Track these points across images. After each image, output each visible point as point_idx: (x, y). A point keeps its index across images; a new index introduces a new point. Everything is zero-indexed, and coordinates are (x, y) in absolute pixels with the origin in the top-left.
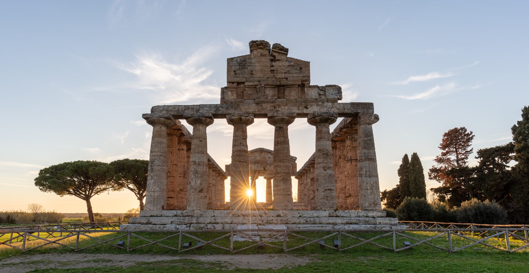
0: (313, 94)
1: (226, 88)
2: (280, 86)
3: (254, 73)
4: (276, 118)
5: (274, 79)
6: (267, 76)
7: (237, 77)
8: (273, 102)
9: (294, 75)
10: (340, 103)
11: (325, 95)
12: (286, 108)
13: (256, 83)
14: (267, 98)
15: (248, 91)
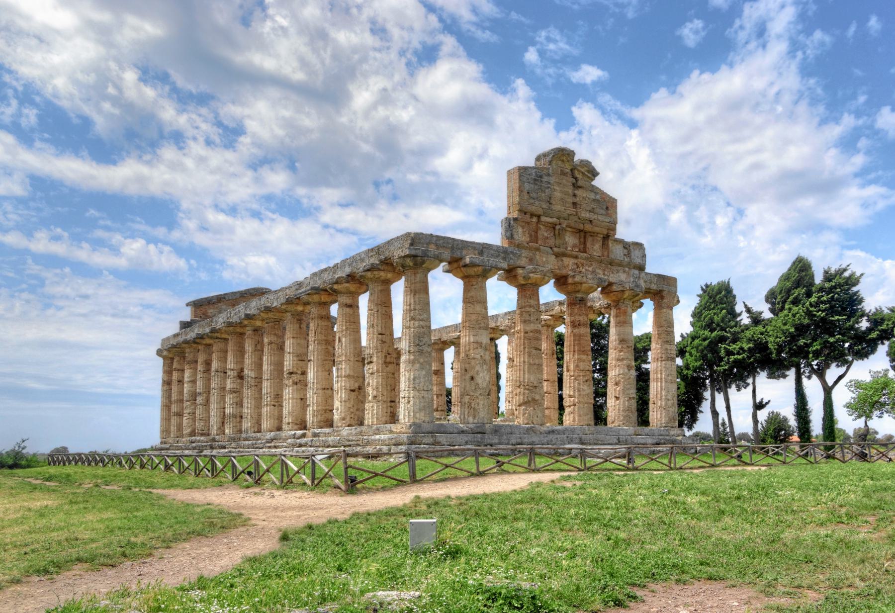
0: (617, 252)
1: (515, 219)
2: (580, 231)
3: (552, 201)
4: (584, 285)
5: (576, 219)
6: (569, 212)
7: (532, 204)
8: (576, 257)
9: (600, 218)
10: (647, 274)
11: (628, 255)
12: (590, 269)
13: (555, 220)
14: (566, 248)
15: (544, 232)
